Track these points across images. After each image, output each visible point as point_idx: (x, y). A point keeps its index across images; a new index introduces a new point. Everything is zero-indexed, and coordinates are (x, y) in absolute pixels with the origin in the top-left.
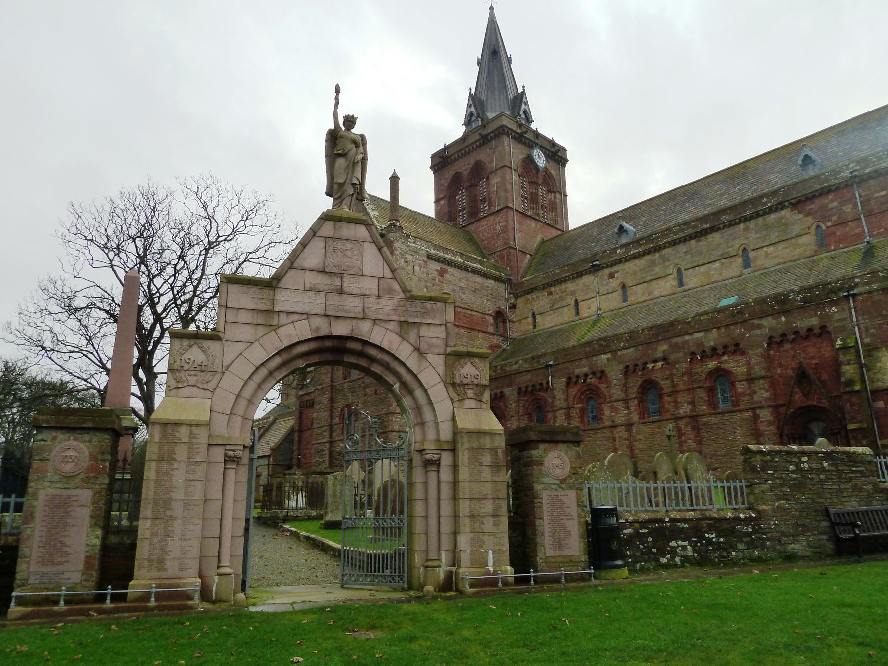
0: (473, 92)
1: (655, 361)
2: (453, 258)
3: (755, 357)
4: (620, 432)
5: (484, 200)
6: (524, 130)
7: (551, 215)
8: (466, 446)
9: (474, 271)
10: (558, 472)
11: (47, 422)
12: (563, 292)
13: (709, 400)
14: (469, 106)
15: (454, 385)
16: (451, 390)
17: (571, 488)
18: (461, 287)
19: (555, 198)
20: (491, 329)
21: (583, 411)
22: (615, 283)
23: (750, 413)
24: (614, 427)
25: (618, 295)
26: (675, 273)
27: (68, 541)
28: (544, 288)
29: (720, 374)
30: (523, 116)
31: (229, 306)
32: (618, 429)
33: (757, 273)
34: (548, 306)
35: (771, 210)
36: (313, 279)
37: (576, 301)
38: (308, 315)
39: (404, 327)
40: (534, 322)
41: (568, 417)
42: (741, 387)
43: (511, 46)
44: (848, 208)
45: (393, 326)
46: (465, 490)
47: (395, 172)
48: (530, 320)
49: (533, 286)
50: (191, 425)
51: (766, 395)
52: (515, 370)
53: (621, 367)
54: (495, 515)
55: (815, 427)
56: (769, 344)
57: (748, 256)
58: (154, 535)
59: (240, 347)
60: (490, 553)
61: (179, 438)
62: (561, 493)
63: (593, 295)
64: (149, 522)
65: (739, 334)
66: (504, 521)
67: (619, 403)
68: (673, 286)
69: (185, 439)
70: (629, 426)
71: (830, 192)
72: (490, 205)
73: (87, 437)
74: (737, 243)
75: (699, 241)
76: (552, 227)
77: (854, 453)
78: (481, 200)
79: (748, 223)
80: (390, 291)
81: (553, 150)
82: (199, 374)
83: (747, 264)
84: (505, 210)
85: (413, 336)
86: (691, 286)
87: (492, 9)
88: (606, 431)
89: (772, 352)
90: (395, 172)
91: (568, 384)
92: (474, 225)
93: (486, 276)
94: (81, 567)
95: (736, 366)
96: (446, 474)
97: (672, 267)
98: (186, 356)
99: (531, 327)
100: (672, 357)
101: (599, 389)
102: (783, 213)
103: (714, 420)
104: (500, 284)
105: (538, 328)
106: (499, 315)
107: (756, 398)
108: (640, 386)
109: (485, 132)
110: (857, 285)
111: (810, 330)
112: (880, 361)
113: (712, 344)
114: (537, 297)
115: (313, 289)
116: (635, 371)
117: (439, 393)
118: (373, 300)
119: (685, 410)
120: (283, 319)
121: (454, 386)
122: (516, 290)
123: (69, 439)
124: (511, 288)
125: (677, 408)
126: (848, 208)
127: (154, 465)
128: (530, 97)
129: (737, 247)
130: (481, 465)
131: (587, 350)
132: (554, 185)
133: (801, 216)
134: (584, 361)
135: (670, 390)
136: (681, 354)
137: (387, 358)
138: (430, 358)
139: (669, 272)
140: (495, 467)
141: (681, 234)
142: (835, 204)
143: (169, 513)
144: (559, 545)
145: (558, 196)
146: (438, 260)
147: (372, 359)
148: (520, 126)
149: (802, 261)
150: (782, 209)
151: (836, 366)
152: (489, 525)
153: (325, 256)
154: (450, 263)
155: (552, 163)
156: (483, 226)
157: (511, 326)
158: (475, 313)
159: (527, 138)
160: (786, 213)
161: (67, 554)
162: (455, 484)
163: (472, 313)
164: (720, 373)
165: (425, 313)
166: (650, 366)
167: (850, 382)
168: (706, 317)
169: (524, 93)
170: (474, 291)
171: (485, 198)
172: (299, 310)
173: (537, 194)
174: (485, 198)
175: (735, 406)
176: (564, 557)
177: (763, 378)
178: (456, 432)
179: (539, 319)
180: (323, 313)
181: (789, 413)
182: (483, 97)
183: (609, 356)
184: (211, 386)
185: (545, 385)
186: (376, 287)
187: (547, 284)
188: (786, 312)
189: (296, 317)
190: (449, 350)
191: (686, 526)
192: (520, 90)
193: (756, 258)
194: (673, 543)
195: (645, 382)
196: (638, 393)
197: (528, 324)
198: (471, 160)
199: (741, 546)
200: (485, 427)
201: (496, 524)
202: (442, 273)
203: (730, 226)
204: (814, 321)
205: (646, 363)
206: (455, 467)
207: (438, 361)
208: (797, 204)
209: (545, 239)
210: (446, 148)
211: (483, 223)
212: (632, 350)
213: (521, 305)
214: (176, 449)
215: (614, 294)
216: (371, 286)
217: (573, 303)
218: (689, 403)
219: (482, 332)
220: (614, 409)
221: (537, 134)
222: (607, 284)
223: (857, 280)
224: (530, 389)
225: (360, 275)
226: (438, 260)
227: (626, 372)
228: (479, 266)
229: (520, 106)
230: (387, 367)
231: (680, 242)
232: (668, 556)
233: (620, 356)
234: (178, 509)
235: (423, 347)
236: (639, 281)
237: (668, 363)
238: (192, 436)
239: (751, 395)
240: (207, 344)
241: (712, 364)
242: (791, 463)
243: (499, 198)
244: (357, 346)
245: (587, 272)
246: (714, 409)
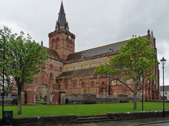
4: (79, 89)
7: (71, 49)
9: (57, 60)
14: (56, 25)
20: (59, 70)
22: (80, 65)
29: (93, 82)
35: (104, 56)
41: (71, 86)
42: (95, 84)
43: (66, 12)
48: (66, 69)
55: (104, 90)
70: (80, 88)
72: (60, 46)
74: (99, 61)
87: (62, 2)
93: (59, 61)
106: (61, 68)
119: (88, 87)
134: (74, 78)
148: (66, 31)
154: (52, 58)
155: (72, 39)
169: (67, 23)
192: (67, 22)
198: (57, 36)
202: (50, 60)
211: (59, 50)
221: (70, 33)
226: (50, 58)
241: (92, 80)
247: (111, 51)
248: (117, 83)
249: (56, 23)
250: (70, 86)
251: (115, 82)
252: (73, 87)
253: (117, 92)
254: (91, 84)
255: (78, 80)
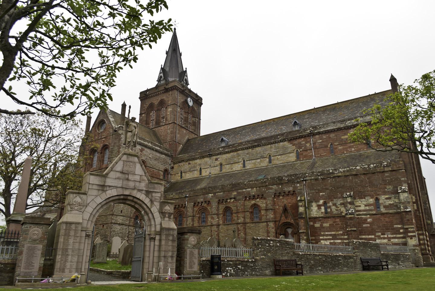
0: (163, 67)
1: (231, 199)
2: (148, 144)
3: (269, 201)
4: (215, 228)
5: (163, 118)
6: (185, 89)
8: (164, 233)
10: (193, 243)
11: (29, 221)
12: (195, 164)
13: (251, 217)
14: (160, 73)
15: (162, 213)
16: (161, 214)
17: (196, 248)
18: (150, 157)
19: (195, 120)
20: (161, 177)
21: (199, 218)
22: (218, 163)
23: (266, 224)
24: (212, 225)
25: (218, 168)
26: (242, 161)
27: (33, 262)
28: (187, 161)
29: (255, 206)
30: (185, 82)
31: (90, 183)
32: (213, 227)
33: (273, 166)
34: (188, 169)
35: (281, 141)
36: (119, 175)
37: (201, 168)
38: (116, 187)
39: (148, 193)
40: (181, 176)
41: (193, 220)
42: (263, 212)
44: (308, 145)
45: (144, 192)
46: (163, 248)
47: (124, 102)
48: (180, 174)
49: (183, 160)
50: (76, 224)
51: (272, 216)
52: (171, 198)
53: (217, 200)
54: (172, 257)
55: (290, 231)
56: (274, 196)
57: (271, 158)
58: (62, 260)
59: (93, 197)
60: (170, 269)
61: (72, 228)
62: (193, 250)
63: (208, 167)
64: (60, 256)
65: (264, 191)
66: (175, 259)
67: (215, 216)
68: (241, 167)
69: (74, 229)
70: (218, 225)
71: (302, 137)
72: (166, 120)
73: (41, 227)
74: (267, 153)
75: (253, 149)
76: (193, 133)
77: (288, 241)
78: (162, 117)
79: (272, 145)
80: (144, 180)
81: (196, 98)
82: (78, 206)
83: (270, 161)
84: (173, 124)
85: (150, 196)
86: (248, 168)
88: (208, 227)
89: (275, 199)
90: (124, 102)
91: (194, 206)
92: (158, 128)
93: (162, 153)
94: (37, 270)
95: (262, 204)
96: (157, 243)
97: (241, 159)
98: (75, 200)
99: (180, 178)
100: (238, 198)
101: (207, 208)
102: (285, 143)
103: (252, 225)
104: (167, 157)
105: (182, 179)
106: (166, 171)
107: (268, 217)
108: (224, 209)
109: (167, 87)
110: (307, 176)
111: (289, 192)
112: (312, 207)
113: (253, 194)
114: (184, 165)
115: (118, 178)
116: (222, 202)
117: (157, 215)
118: (138, 183)
120: (108, 188)
121: (162, 213)
122: (174, 160)
123: (35, 227)
124: (172, 159)
125: (238, 219)
126: (308, 145)
127: (63, 237)
128: (189, 73)
129: (267, 154)
130: (169, 240)
131: (204, 191)
132: (195, 114)
133: (291, 145)
134: (202, 196)
135: (236, 211)
136: (241, 197)
137: (141, 203)
138: (155, 203)
139: (240, 161)
140: (173, 241)
141: (246, 146)
142: (304, 142)
143: (67, 253)
144: (191, 267)
145: (197, 119)
146: (140, 144)
147: (136, 203)
148: (183, 86)
149: (290, 163)
150: (285, 141)
151: (296, 207)
152: (170, 260)
153: (123, 167)
154: (146, 146)
156: (162, 129)
157: (171, 176)
158: (155, 170)
159: (185, 92)
160: (286, 143)
161: (33, 266)
162: (160, 246)
163: (154, 170)
164: (256, 206)
165: (154, 188)
166: (229, 201)
167: (301, 213)
168: (252, 182)
169: (186, 71)
170: (156, 160)
171: (164, 117)
172: (113, 185)
173: (188, 117)
174: (164, 117)
175: (260, 220)
176: (193, 271)
177: (271, 209)
178: (162, 228)
179: (183, 175)
180: (121, 186)
181: (280, 224)
182: (167, 69)
183: (213, 195)
184: (82, 210)
185: (184, 206)
186: (139, 178)
187: (189, 159)
188: (282, 184)
189: (112, 188)
190: (161, 201)
191: (232, 263)
192: (184, 70)
193: (274, 159)
194: (227, 269)
195: (226, 207)
196: (223, 212)
197: (179, 176)
198: (159, 98)
199: (249, 271)
200: (171, 227)
201: (172, 259)
202: (142, 150)
203: (265, 145)
204: (291, 189)
205: (227, 199)
206: (160, 240)
207: (157, 204)
208: (290, 140)
209: (190, 138)
210: (148, 90)
211: (162, 128)
212: (222, 193)
213: (176, 168)
214: (71, 232)
215: (217, 167)
216: (137, 178)
217: (199, 169)
218: (243, 217)
219: (157, 178)
220: (212, 218)
221: (190, 91)
222: (214, 163)
223: (307, 175)
224: (177, 207)
225: (134, 174)
226: (140, 144)
227: (219, 202)
228: (159, 149)
229: (184, 77)
230: (141, 206)
231: (245, 149)
232: (225, 273)
233: (217, 195)
234: (70, 252)
235: (153, 199)
236: (227, 163)
237: (236, 200)
238: (76, 227)
239: (266, 216)
240: (82, 196)
241: (253, 202)
242: (267, 243)
243: (170, 118)
244: (131, 198)
245: (207, 156)
246: (252, 220)
247: (297, 128)
248: (329, 210)
249: (158, 70)
250: (190, 219)
251: (323, 208)
252: (199, 223)
253: (330, 235)
254: (251, 212)
255: (214, 204)
